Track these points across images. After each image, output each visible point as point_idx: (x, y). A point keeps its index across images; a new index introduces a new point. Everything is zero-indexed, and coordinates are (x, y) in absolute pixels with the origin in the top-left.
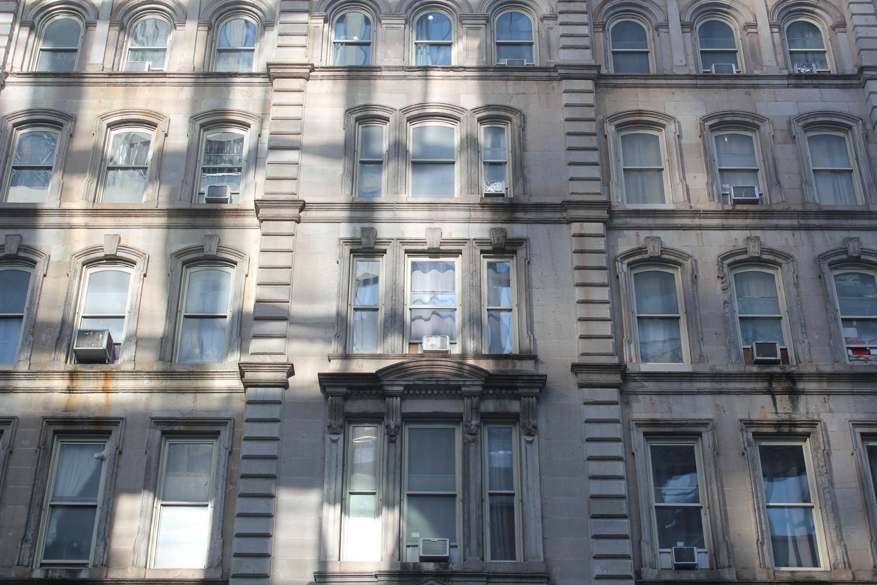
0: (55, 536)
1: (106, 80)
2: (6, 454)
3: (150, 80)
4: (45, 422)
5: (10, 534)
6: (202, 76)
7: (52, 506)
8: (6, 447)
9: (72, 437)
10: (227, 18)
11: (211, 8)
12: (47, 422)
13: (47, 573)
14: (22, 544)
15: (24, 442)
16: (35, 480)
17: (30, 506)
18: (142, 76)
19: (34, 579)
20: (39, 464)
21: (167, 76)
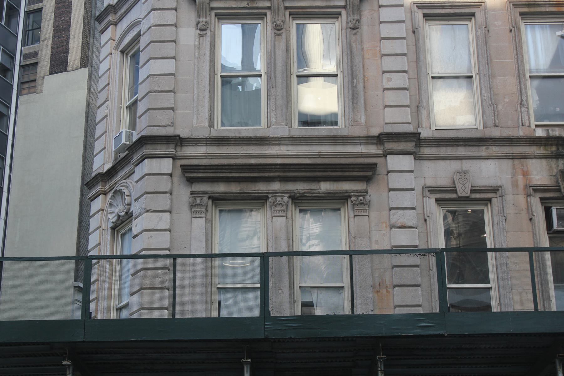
0: (538, 102)
2: (485, 32)
4: (511, 5)
5: (507, 100)
7: (530, 77)
8: (483, 27)
9: (530, 18)
12: (513, 5)
13: (548, 133)
14: (521, 108)
15: (496, 23)
16: (517, 54)
17: (519, 76)
19: (537, 136)
20: (517, 40)
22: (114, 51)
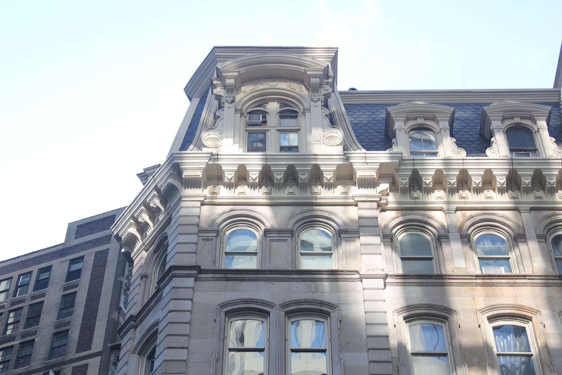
1: (474, 281)
3: (512, 281)
6: (558, 278)
10: (553, 233)
11: (542, 225)
18: (505, 278)
21: (527, 278)
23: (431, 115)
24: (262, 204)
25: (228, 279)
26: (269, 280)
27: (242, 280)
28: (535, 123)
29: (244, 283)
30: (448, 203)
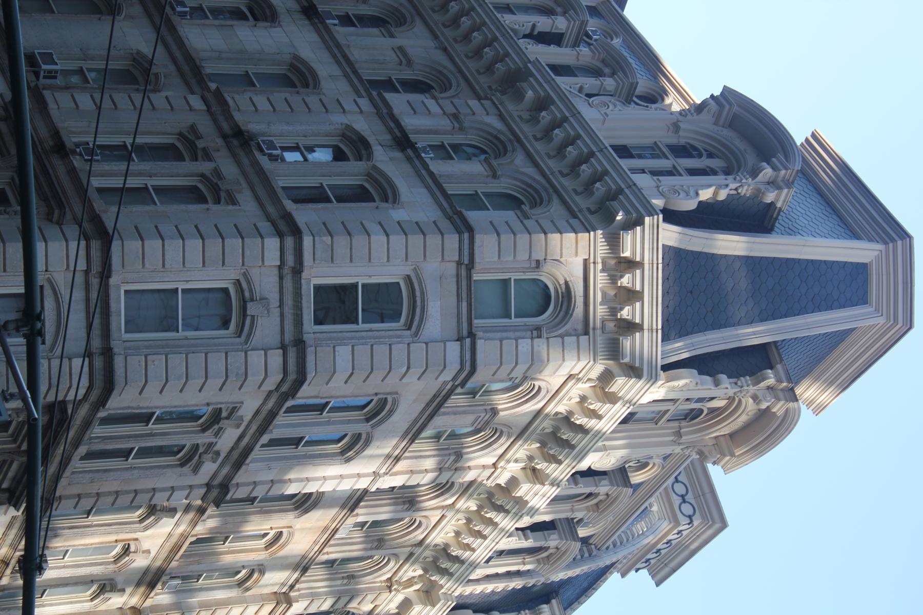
22: (47, 276)
23: (602, 507)
24: (562, 388)
25: (435, 397)
26: (416, 421)
27: (428, 405)
28: (538, 561)
29: (423, 405)
30: (458, 511)
